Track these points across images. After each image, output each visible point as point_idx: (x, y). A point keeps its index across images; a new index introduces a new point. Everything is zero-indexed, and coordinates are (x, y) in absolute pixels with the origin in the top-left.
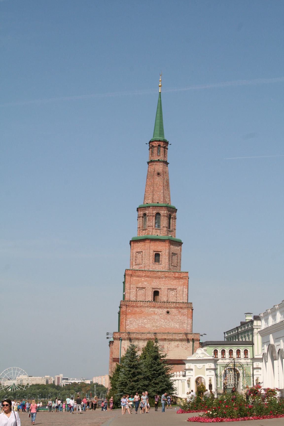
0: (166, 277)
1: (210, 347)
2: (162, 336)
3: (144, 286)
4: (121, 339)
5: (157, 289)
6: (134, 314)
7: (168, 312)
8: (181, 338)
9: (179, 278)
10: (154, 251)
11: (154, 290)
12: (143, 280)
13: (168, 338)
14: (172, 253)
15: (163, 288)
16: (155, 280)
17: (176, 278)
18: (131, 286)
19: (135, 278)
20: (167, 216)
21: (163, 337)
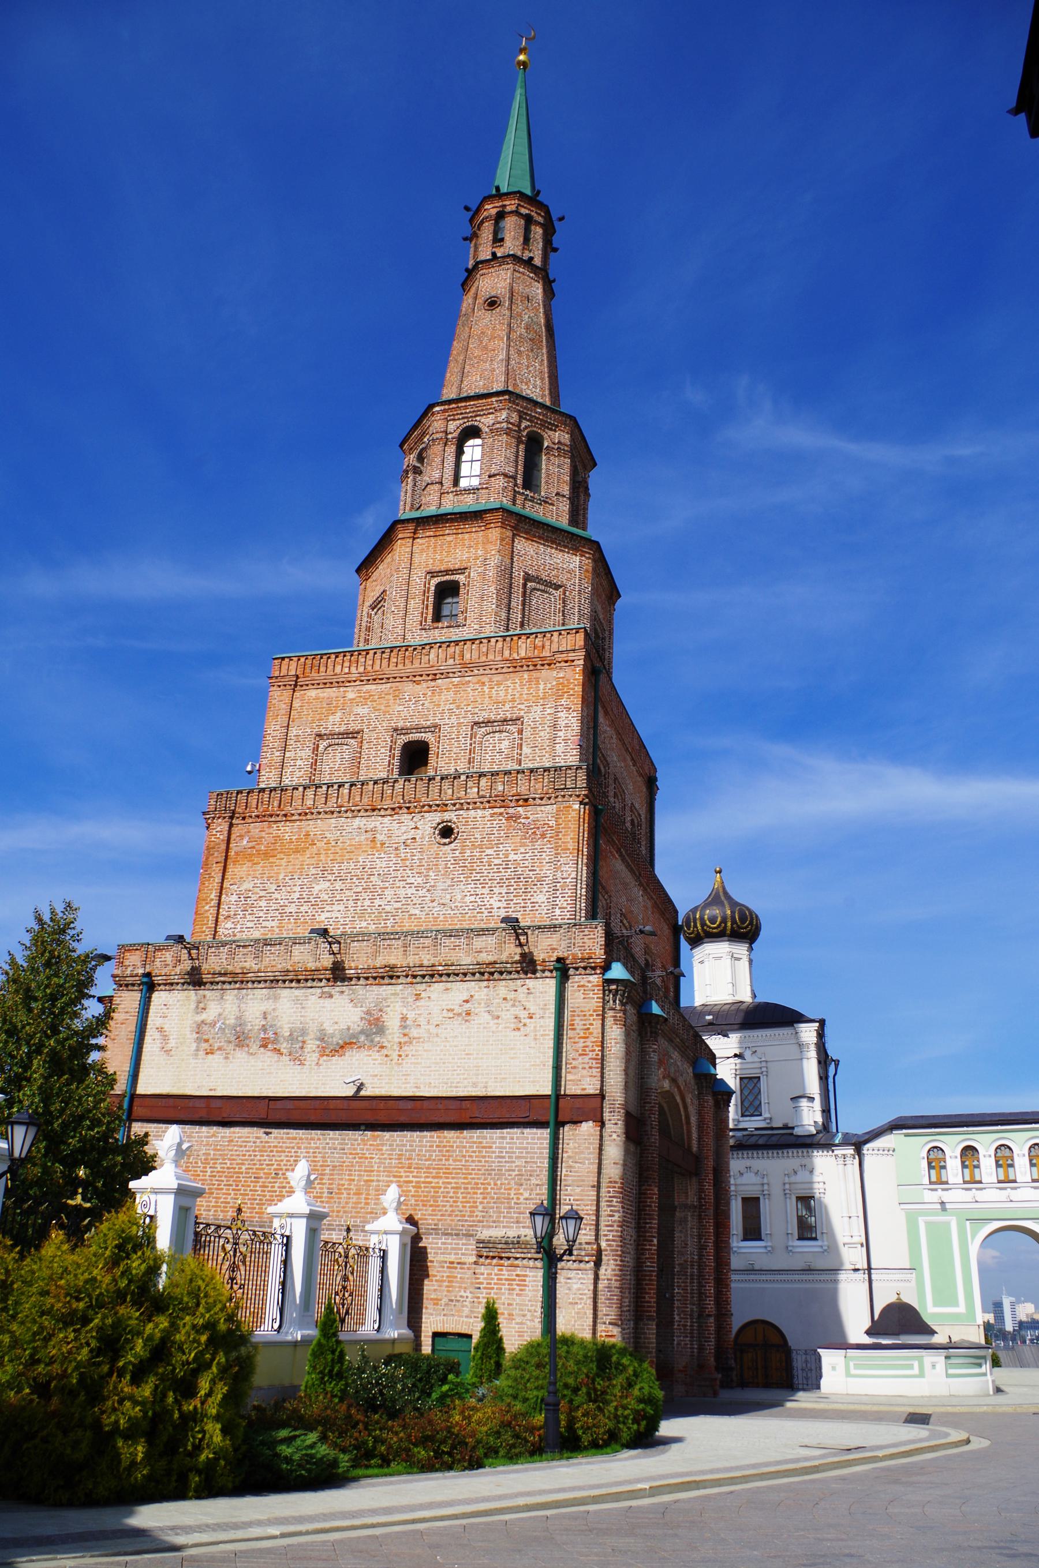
0: (467, 667)
1: (906, 1135)
2: (376, 954)
3: (354, 726)
4: (149, 985)
5: (418, 729)
6: (267, 855)
7: (447, 832)
8: (490, 958)
9: (533, 664)
10: (432, 574)
11: (403, 739)
12: (351, 695)
13: (412, 960)
14: (528, 578)
15: (448, 722)
16: (409, 688)
17: (516, 666)
18: (293, 732)
19: (312, 693)
20: (508, 432)
21: (380, 961)
